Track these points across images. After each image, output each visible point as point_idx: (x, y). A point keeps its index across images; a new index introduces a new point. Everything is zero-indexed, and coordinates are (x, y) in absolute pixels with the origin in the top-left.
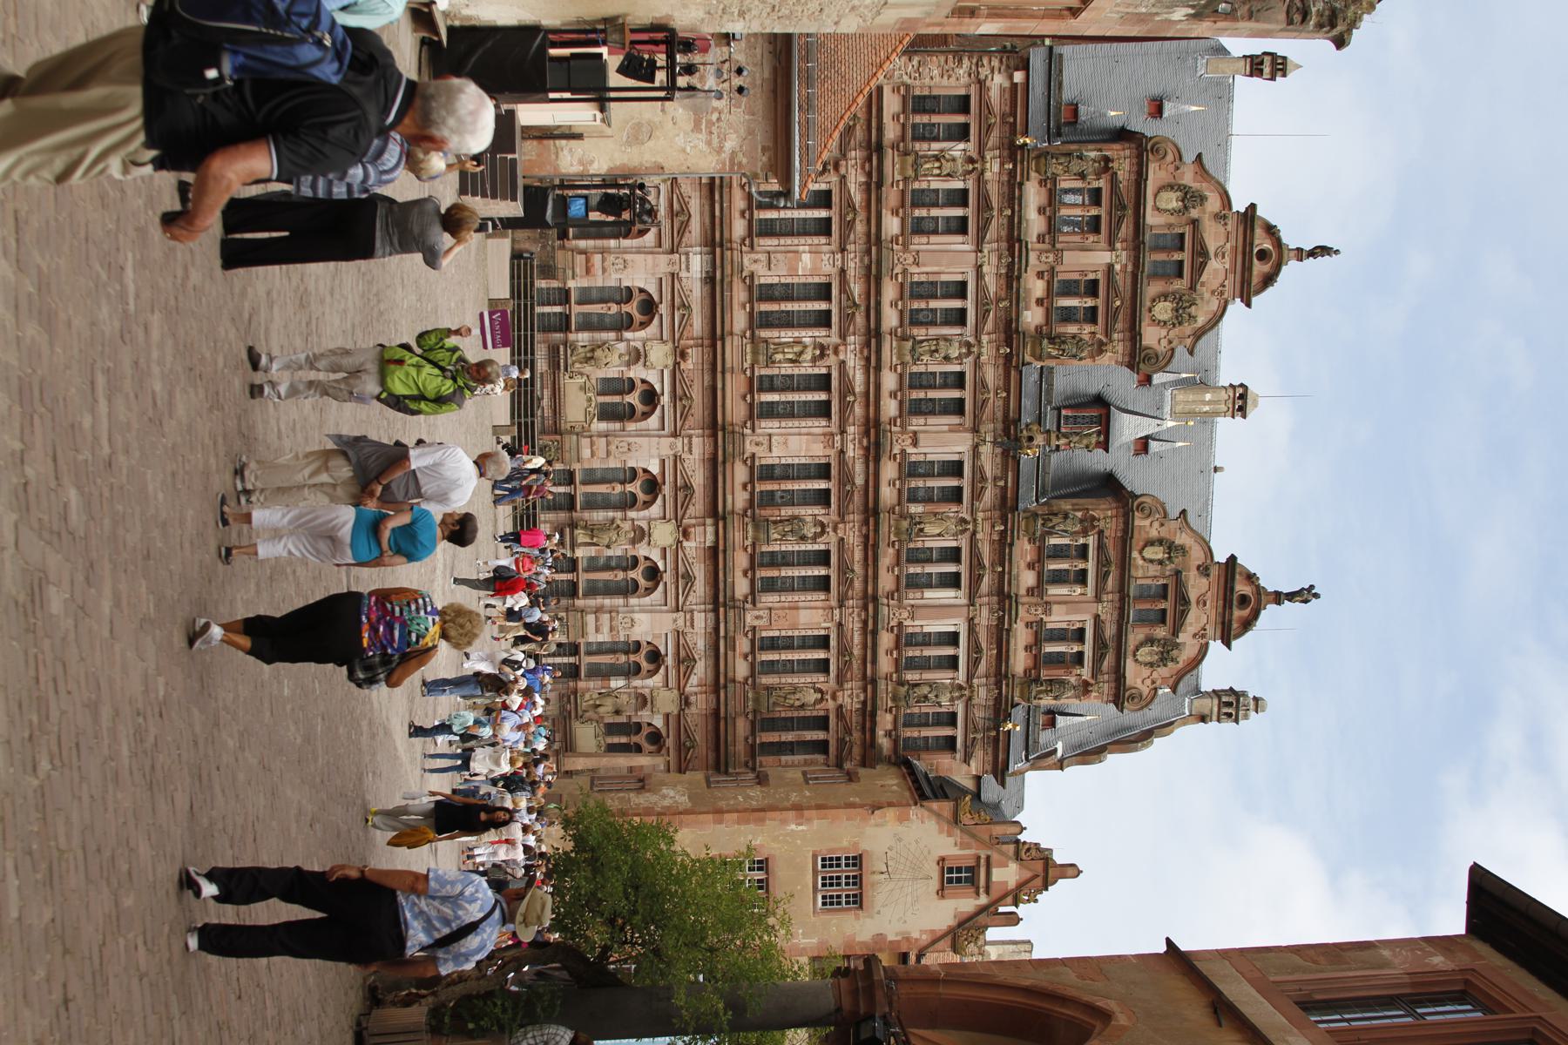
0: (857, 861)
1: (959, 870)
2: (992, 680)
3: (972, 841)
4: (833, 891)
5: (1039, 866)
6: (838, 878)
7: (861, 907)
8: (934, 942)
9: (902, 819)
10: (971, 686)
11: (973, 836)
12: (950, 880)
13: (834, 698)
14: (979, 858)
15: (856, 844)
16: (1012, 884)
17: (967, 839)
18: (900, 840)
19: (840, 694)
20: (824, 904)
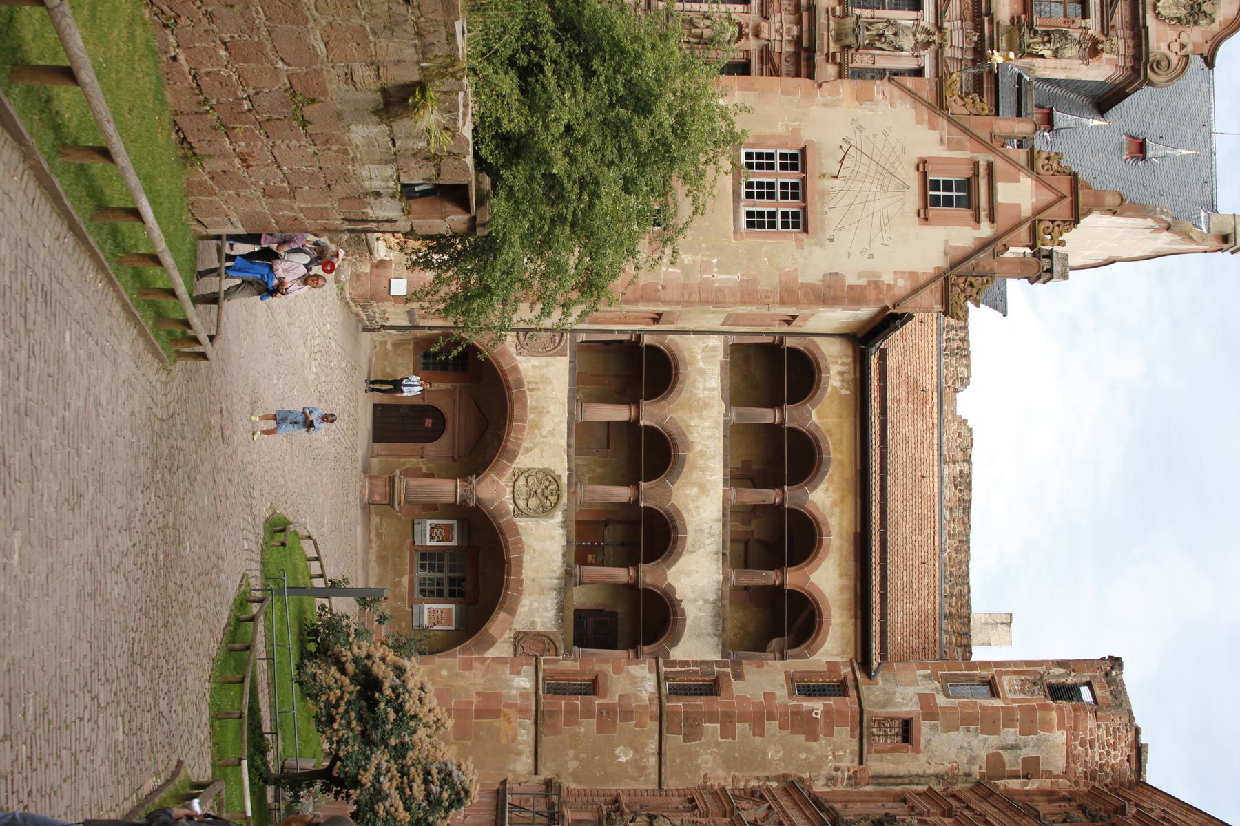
0: (796, 161)
1: (948, 185)
2: (969, 24)
3: (965, 139)
4: (764, 205)
5: (1064, 186)
6: (772, 214)
7: (805, 230)
8: (915, 291)
9: (863, 98)
10: (940, 29)
11: (966, 131)
12: (936, 201)
13: (757, 35)
14: (976, 165)
15: (796, 131)
16: (1026, 210)
17: (957, 135)
18: (860, 129)
19: (764, 25)
20: (750, 224)
